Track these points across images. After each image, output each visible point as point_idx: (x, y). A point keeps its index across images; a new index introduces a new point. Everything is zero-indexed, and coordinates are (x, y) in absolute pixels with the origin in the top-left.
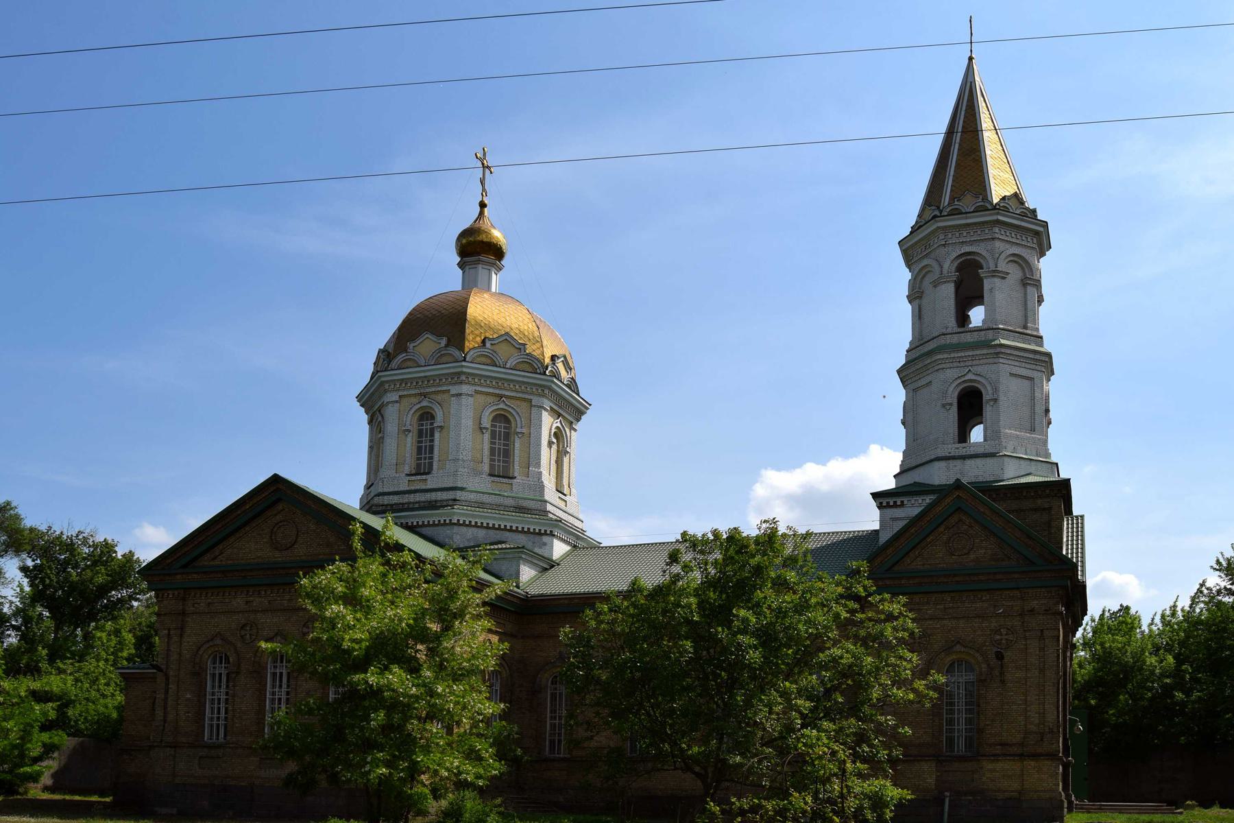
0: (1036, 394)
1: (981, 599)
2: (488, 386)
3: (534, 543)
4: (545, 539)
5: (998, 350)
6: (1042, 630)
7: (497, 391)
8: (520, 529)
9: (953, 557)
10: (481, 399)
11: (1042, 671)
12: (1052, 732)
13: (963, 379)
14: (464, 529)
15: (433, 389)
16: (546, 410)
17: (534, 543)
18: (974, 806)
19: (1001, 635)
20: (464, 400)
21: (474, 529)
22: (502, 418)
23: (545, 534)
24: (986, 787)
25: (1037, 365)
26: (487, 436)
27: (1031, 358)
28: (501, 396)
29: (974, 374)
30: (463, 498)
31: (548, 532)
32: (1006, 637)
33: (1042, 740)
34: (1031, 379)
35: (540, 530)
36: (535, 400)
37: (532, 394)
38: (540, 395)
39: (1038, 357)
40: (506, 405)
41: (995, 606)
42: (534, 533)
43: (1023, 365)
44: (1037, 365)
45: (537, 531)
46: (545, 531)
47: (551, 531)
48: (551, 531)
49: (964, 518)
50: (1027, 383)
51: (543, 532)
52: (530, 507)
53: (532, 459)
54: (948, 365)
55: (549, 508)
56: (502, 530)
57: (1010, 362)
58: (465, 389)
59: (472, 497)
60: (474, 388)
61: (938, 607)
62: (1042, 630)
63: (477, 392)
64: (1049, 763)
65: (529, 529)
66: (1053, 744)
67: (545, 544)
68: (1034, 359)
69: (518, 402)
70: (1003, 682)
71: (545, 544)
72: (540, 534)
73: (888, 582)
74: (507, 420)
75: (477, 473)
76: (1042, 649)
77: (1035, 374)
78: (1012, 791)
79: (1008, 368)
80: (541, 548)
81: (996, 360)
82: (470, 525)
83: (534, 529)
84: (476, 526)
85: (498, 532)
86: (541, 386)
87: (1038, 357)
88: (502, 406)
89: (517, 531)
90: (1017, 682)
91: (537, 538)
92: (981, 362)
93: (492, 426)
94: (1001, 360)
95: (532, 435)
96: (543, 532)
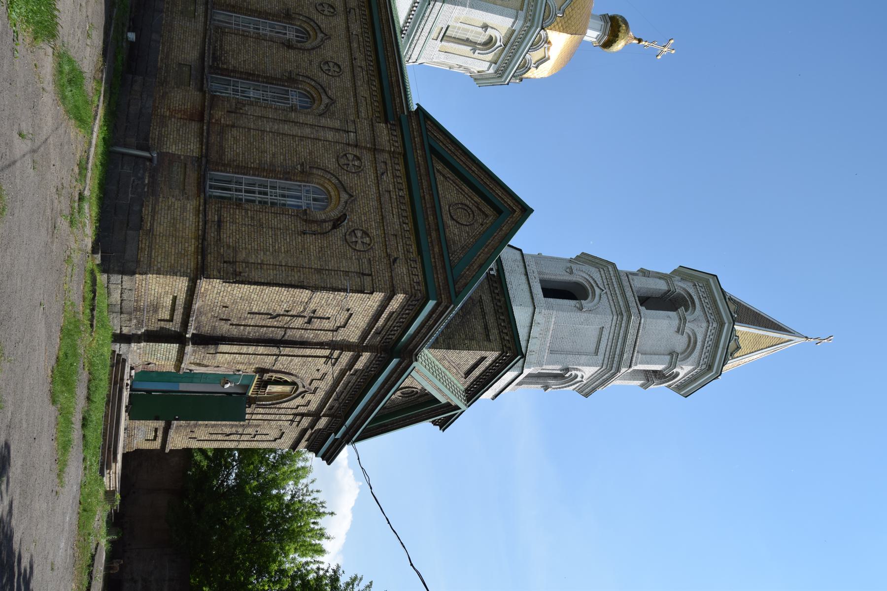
0: (584, 357)
1: (404, 223)
5: (625, 314)
11: (319, 271)
12: (236, 275)
13: (594, 285)
16: (514, 23)
19: (362, 237)
25: (609, 359)
27: (615, 352)
32: (360, 242)
33: (225, 262)
34: (596, 353)
36: (522, 14)
37: (527, 10)
39: (616, 359)
41: (396, 235)
43: (610, 344)
44: (609, 359)
50: (592, 347)
54: (603, 275)
55: (438, 4)
57: (613, 328)
61: (391, 185)
62: (370, 275)
64: (192, 265)
66: (220, 273)
68: (615, 354)
70: (304, 233)
76: (346, 273)
77: (600, 357)
79: (607, 326)
81: (614, 313)
86: (534, 19)
87: (616, 359)
92: (611, 302)
94: (615, 318)
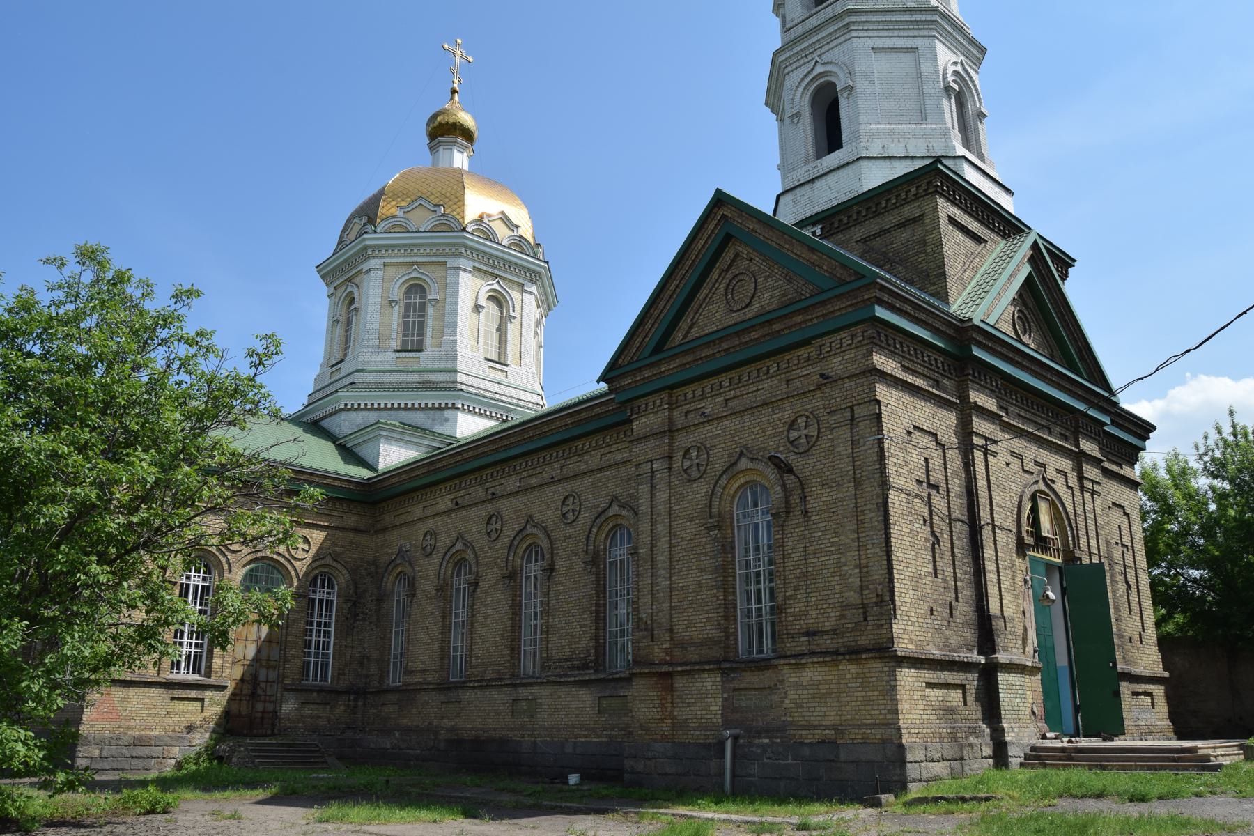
0: (924, 68)
1: (768, 372)
2: (397, 256)
3: (433, 420)
4: (447, 414)
5: (847, 20)
6: (852, 408)
7: (408, 260)
8: (416, 406)
9: (733, 315)
10: (391, 271)
11: (858, 483)
12: (882, 601)
13: (811, 76)
14: (353, 414)
15: (354, 272)
16: (465, 270)
17: (433, 420)
18: (770, 758)
19: (799, 429)
20: (372, 275)
21: (364, 413)
22: (416, 288)
23: (447, 407)
24: (789, 719)
25: (920, 29)
26: (397, 311)
27: (907, 21)
28: (411, 264)
29: (822, 64)
30: (361, 380)
31: (450, 405)
32: (805, 432)
33: (865, 620)
34: (914, 50)
35: (440, 404)
36: (451, 262)
37: (446, 255)
38: (455, 256)
39: (918, 17)
40: (420, 273)
41: (788, 381)
42: (433, 409)
43: (896, 33)
44: (920, 29)
45: (436, 406)
46: (447, 404)
47: (453, 404)
48: (453, 404)
49: (741, 249)
50: (907, 58)
51: (443, 406)
52: (435, 380)
53: (449, 326)
54: (794, 66)
55: (460, 378)
56: (396, 409)
57: (871, 33)
58: (373, 263)
59: (371, 377)
60: (383, 261)
61: (717, 400)
62: (852, 408)
63: (385, 265)
64: (876, 665)
65: (426, 404)
66: (882, 625)
67: (447, 420)
68: (911, 21)
69: (433, 267)
70: (806, 513)
71: (447, 420)
72: (440, 409)
73: (647, 374)
74: (423, 290)
75: (380, 350)
76: (855, 444)
77: (918, 42)
78: (827, 727)
79: (869, 43)
80: (442, 425)
81: (847, 36)
82: (359, 409)
83: (433, 404)
84: (366, 409)
85: (392, 412)
86: (454, 245)
87: (918, 17)
88: (415, 275)
89: (413, 409)
90: (825, 511)
91: (438, 414)
92: (831, 45)
93: (406, 298)
94: (854, 34)
95: (447, 300)
96: (443, 406)
